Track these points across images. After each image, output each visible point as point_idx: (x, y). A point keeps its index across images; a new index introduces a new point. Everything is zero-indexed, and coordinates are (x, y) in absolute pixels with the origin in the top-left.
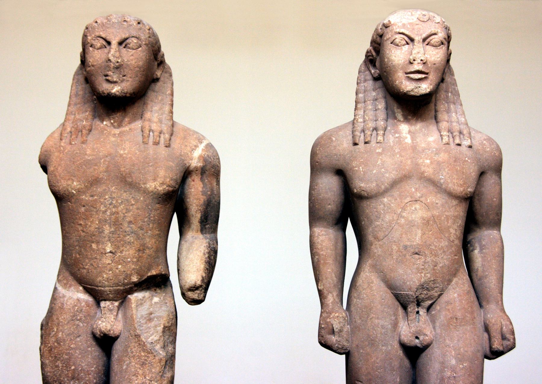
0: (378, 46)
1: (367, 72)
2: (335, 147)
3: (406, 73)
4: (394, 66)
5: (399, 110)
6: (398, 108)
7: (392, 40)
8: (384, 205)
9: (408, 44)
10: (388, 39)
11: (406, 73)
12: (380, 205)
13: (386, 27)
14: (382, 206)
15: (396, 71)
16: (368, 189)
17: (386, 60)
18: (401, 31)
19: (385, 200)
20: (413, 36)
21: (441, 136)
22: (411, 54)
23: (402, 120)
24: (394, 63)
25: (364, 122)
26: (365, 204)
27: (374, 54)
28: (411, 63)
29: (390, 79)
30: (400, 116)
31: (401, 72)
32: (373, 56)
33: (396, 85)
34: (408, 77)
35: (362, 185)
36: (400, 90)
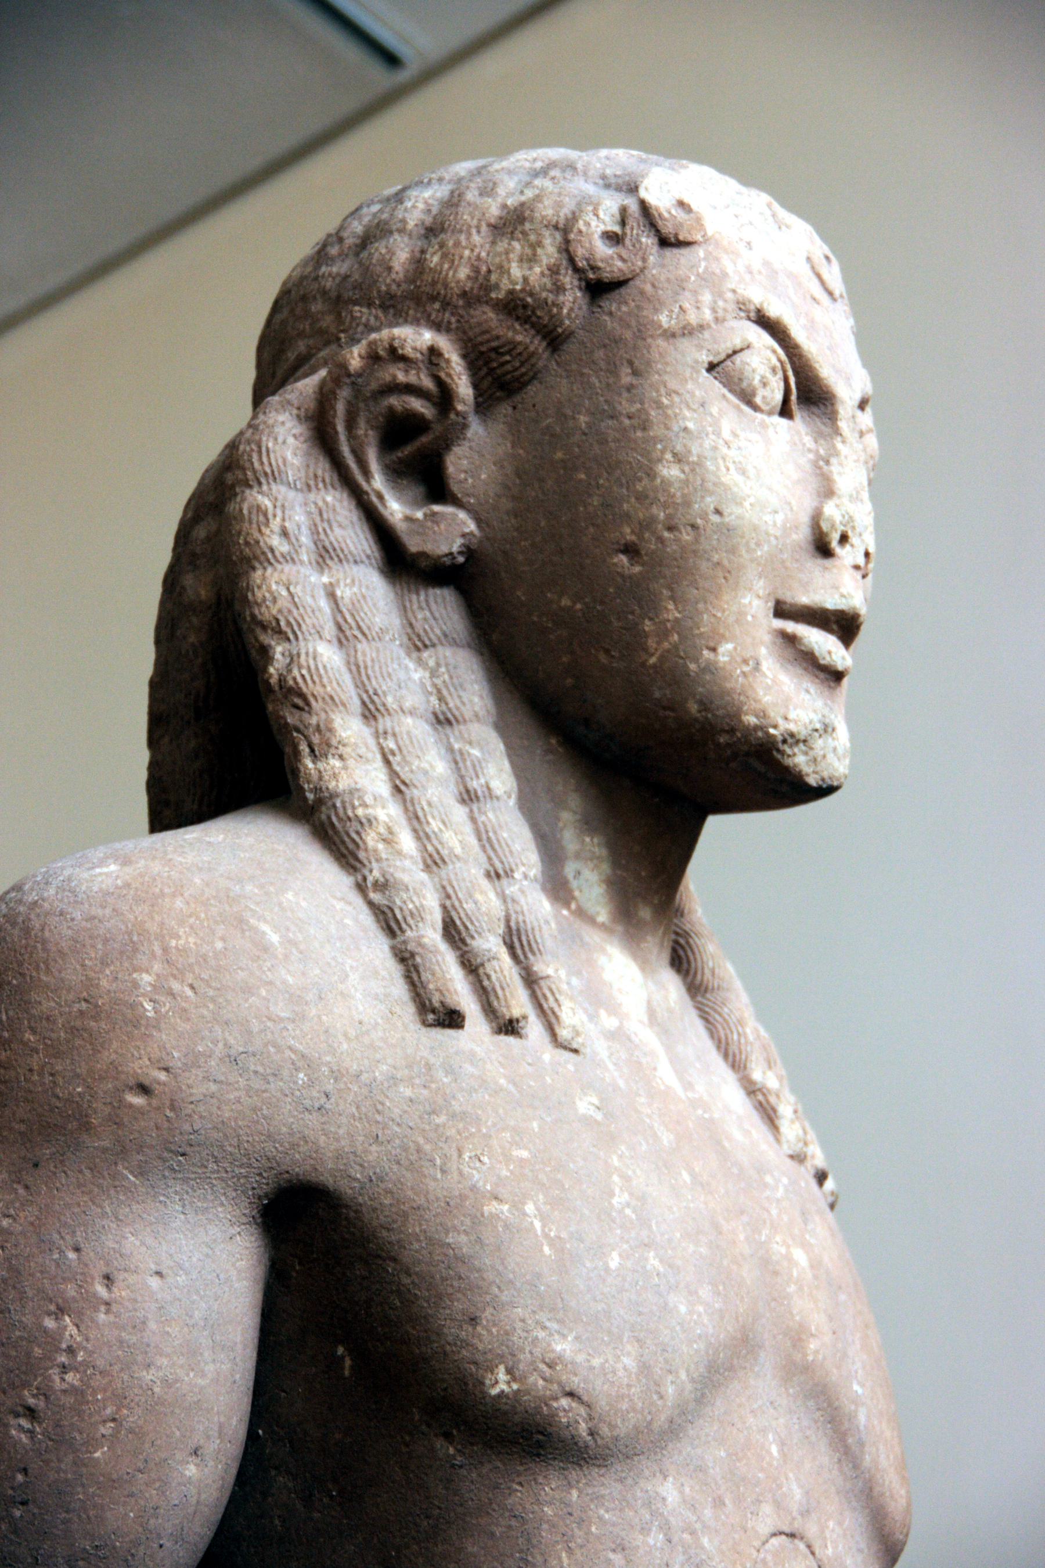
0: (538, 345)
1: (336, 502)
2: (295, 998)
3: (781, 611)
4: (728, 530)
5: (594, 845)
6: (587, 825)
7: (725, 347)
8: (666, 1527)
9: (785, 411)
10: (688, 331)
11: (781, 611)
12: (645, 1530)
13: (664, 242)
14: (656, 1539)
15: (730, 574)
16: (599, 1390)
17: (670, 471)
18: (773, 311)
19: (670, 1492)
20: (827, 371)
21: (752, 1089)
22: (827, 491)
23: (603, 917)
24: (733, 514)
25: (433, 862)
26: (551, 1498)
27: (464, 388)
28: (823, 549)
29: (671, 612)
30: (591, 885)
31: (760, 586)
32: (444, 397)
33: (710, 668)
34: (791, 640)
35: (563, 1347)
36: (737, 715)
